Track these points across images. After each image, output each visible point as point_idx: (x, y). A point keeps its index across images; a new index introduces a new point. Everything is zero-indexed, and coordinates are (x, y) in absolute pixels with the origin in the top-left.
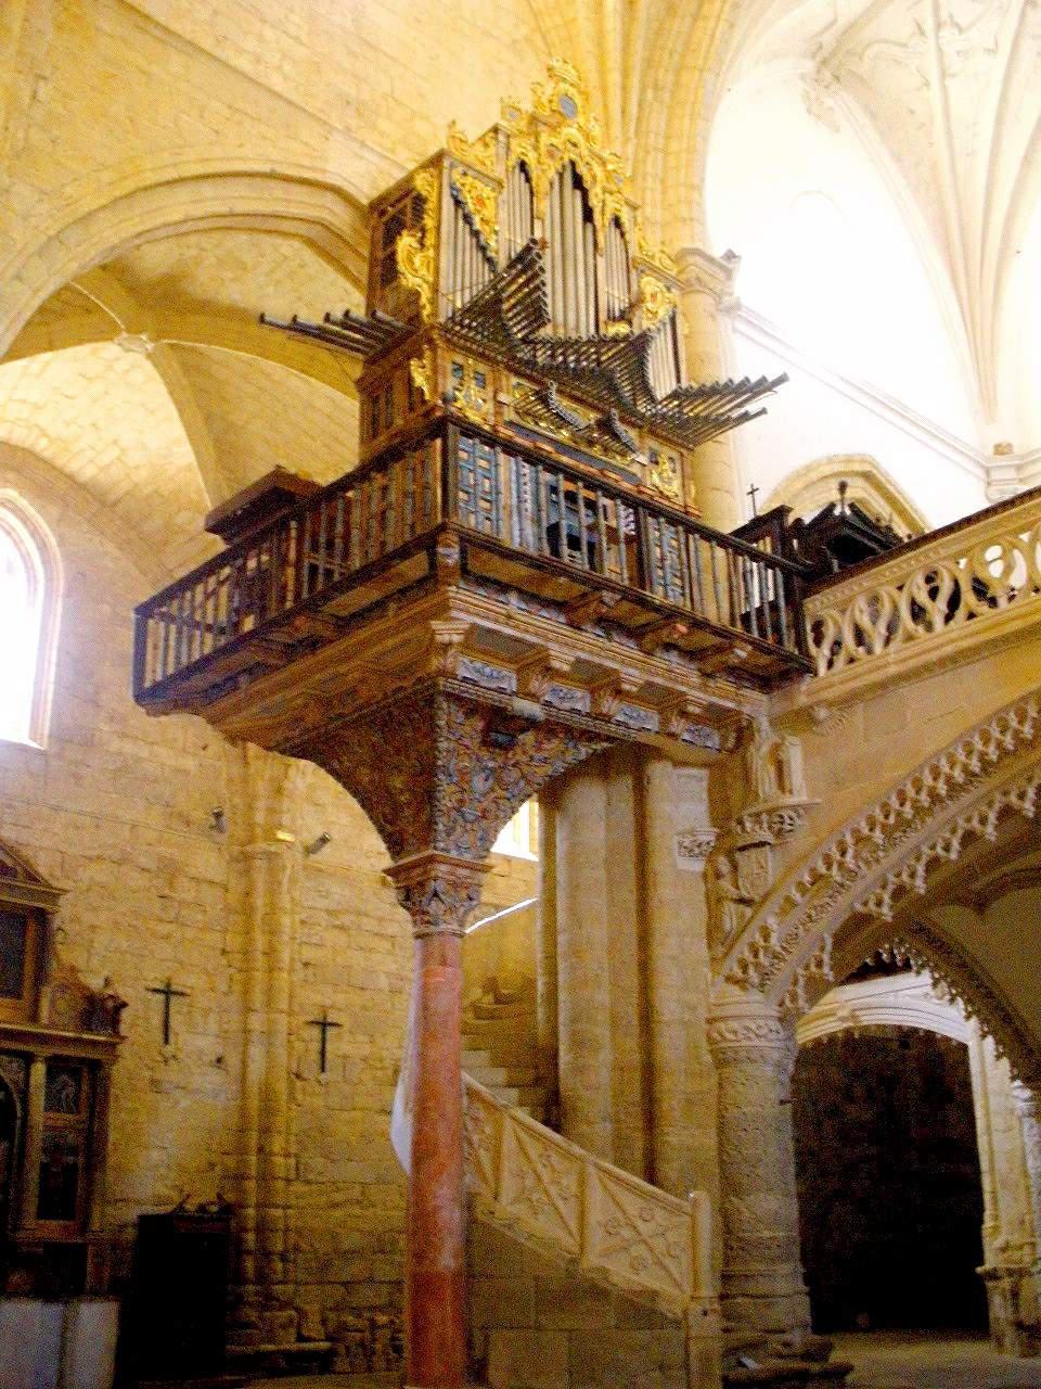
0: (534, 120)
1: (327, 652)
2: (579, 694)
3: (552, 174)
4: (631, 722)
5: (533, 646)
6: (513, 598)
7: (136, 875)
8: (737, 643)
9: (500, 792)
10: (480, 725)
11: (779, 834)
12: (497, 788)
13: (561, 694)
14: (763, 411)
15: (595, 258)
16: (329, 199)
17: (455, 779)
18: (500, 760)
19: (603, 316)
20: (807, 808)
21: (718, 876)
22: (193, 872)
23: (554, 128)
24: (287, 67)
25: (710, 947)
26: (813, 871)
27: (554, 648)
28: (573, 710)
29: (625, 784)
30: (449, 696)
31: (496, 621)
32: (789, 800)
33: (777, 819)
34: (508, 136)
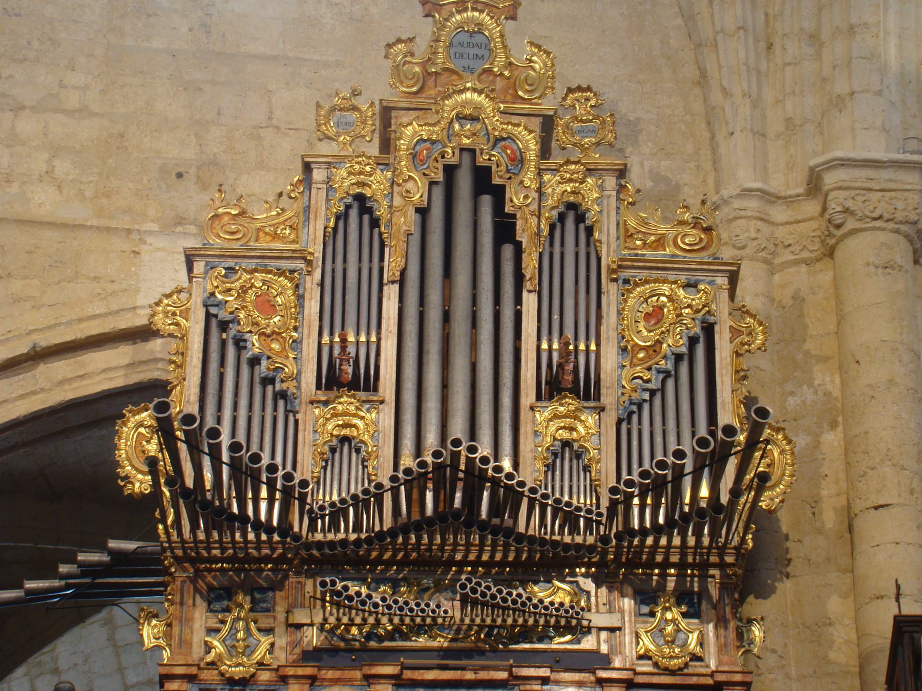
15: (518, 300)
19: (528, 396)
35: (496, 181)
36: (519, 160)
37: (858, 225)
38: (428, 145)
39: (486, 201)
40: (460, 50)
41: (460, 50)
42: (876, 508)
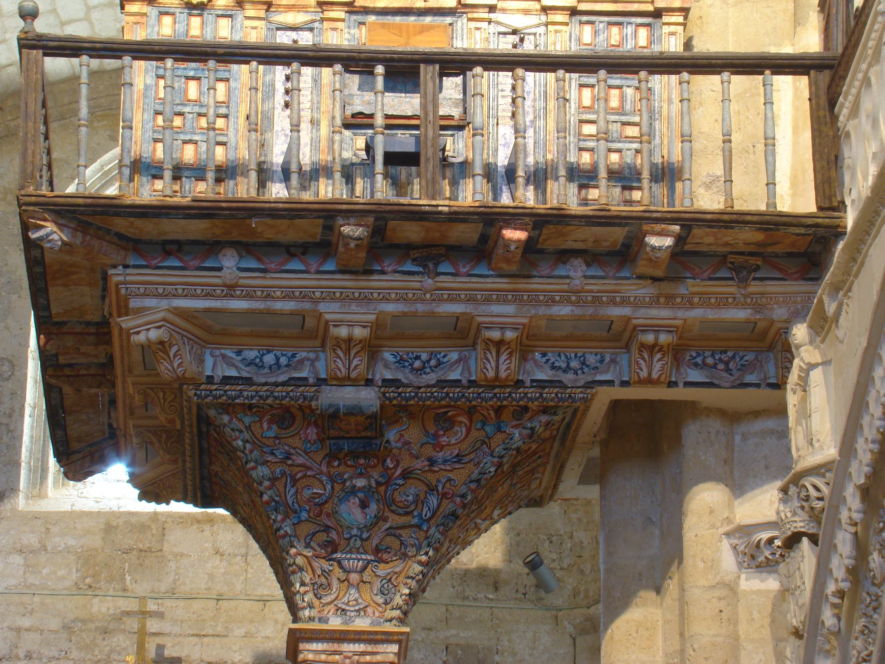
2: (454, 356)
4: (568, 378)
6: (229, 261)
12: (387, 514)
13: (417, 364)
17: (304, 515)
27: (330, 310)
28: (442, 383)
31: (208, 295)
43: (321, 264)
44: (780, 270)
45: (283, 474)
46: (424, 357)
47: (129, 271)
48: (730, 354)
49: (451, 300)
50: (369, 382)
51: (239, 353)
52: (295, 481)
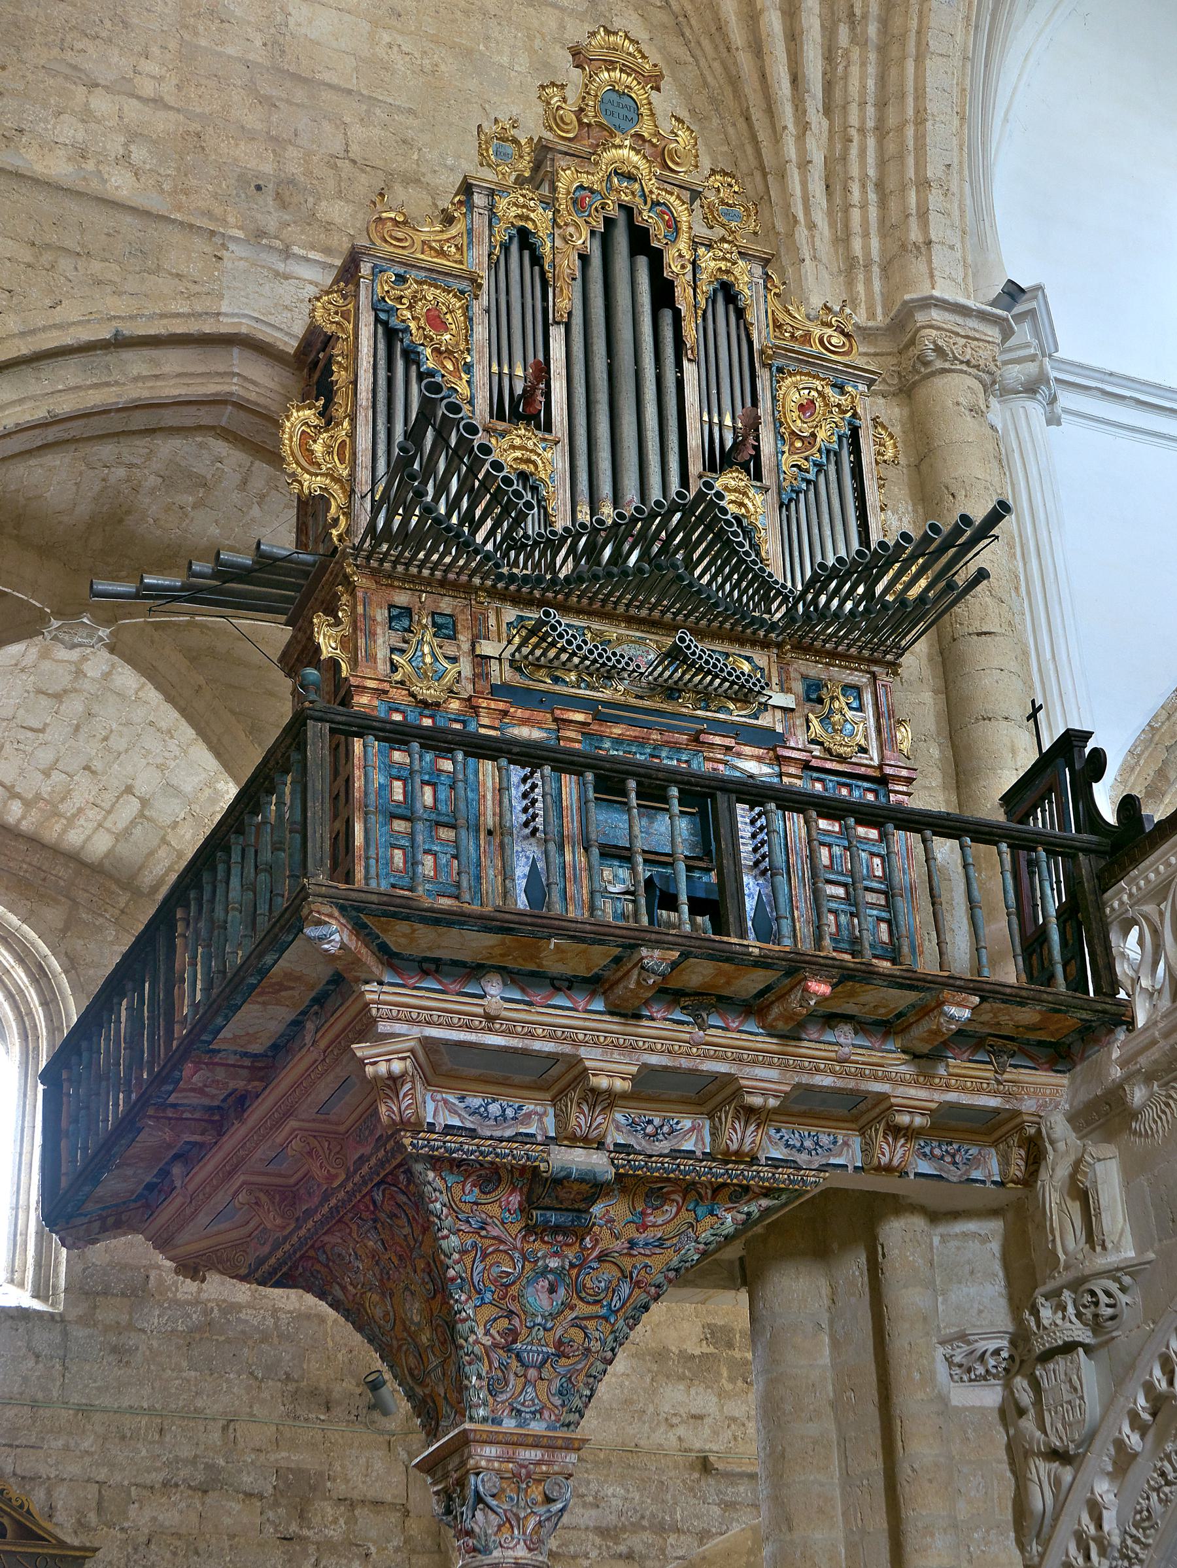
0: (542, 152)
1: (258, 1112)
2: (687, 1124)
3: (582, 239)
4: (802, 1158)
5: (554, 1058)
6: (494, 989)
7: (236, 1506)
8: (946, 994)
9: (583, 1309)
10: (515, 1200)
11: (1096, 1325)
12: (575, 1301)
13: (650, 1129)
14: (982, 575)
15: (679, 366)
16: (238, 361)
18: (571, 1254)
20: (1131, 1269)
21: (1021, 1412)
22: (341, 1489)
23: (585, 159)
24: (139, 154)
25: (1021, 1546)
26: (1149, 1387)
27: (591, 1056)
28: (675, 1154)
29: (854, 1266)
30: (435, 1162)
31: (468, 1027)
32: (1103, 1261)
33: (1088, 1298)
34: (492, 193)
35: (655, 244)
36: (674, 226)
37: (947, 365)
38: (587, 193)
39: (642, 262)
40: (609, 106)
41: (609, 106)
42: (979, 634)
43: (588, 1003)
44: (1032, 1058)
45: (474, 1245)
46: (657, 1121)
47: (385, 989)
48: (955, 1146)
49: (716, 1058)
50: (601, 1145)
51: (462, 1099)
52: (485, 1256)
